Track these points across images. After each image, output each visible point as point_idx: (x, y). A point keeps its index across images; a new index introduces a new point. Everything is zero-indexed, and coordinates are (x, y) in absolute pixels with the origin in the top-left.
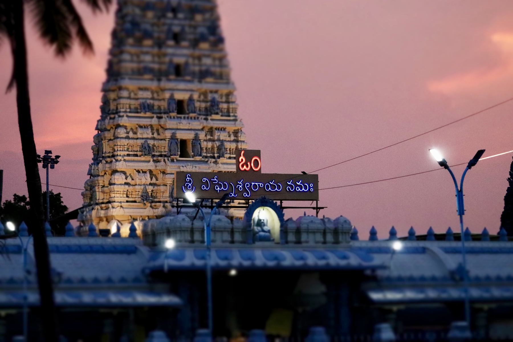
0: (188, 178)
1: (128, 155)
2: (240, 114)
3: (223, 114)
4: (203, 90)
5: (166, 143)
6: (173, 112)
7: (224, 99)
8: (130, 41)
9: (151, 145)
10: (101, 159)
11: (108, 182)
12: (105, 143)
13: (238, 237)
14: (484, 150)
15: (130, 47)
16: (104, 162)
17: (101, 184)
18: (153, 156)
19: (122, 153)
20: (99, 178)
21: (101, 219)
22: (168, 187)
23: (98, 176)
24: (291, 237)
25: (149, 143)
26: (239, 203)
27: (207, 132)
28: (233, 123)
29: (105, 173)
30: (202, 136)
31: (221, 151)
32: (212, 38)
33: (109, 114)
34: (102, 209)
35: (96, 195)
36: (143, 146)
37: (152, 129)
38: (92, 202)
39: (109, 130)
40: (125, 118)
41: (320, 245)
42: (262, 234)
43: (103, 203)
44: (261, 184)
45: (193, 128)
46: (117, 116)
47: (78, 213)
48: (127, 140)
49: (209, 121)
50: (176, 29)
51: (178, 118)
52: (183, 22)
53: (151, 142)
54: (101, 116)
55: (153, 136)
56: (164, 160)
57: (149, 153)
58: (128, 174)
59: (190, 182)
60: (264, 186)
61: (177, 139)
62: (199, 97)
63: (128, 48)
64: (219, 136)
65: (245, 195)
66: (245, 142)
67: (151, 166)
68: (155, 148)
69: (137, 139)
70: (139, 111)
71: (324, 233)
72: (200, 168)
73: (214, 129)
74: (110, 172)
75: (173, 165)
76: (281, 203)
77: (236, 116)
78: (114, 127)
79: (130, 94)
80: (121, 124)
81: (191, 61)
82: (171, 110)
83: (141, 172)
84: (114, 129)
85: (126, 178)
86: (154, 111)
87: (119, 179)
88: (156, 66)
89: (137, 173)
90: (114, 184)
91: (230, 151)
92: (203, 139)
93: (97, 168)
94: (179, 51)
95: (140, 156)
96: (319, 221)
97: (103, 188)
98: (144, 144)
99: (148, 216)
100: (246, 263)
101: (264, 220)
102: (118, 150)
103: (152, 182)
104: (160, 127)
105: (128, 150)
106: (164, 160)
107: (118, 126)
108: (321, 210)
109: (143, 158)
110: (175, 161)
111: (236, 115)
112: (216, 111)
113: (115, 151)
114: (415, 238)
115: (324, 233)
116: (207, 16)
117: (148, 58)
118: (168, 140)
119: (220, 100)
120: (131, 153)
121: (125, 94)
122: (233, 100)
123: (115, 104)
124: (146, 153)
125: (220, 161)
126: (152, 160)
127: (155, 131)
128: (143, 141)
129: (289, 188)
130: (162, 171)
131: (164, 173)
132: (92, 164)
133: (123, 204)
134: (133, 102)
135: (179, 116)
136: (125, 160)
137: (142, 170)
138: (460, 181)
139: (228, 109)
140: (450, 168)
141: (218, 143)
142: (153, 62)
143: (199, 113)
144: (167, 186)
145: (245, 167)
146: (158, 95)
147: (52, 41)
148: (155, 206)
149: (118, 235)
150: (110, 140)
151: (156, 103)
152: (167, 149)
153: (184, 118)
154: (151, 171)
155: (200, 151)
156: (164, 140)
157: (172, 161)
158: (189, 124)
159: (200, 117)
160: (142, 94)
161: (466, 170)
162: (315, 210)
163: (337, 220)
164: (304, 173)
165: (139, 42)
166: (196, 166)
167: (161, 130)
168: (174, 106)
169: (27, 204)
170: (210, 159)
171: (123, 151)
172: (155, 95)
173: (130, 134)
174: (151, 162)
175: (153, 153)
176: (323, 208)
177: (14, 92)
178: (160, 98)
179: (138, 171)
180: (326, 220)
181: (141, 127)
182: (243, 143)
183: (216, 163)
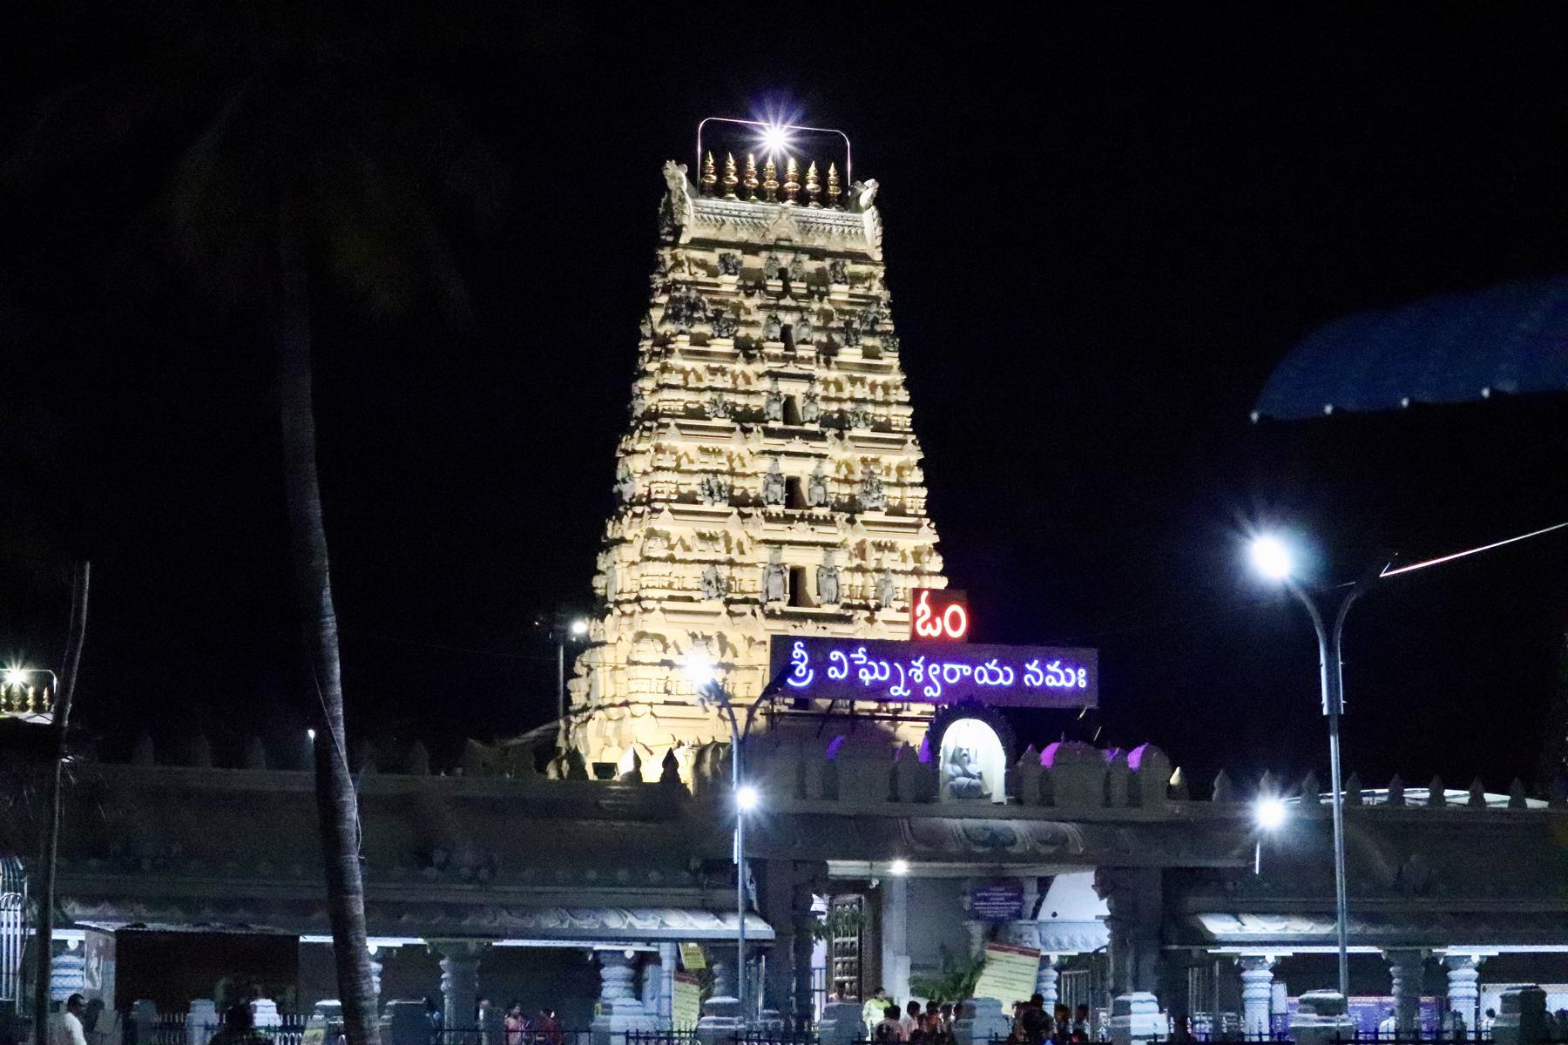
1: (672, 598)
5: (758, 574)
6: (776, 503)
10: (611, 606)
11: (625, 661)
16: (617, 612)
18: (728, 602)
23: (602, 644)
25: (719, 571)
26: (922, 713)
28: (914, 530)
33: (632, 505)
40: (666, 514)
42: (964, 780)
43: (612, 705)
49: (859, 524)
50: (788, 319)
53: (724, 572)
55: (728, 556)
58: (669, 641)
59: (802, 659)
62: (838, 471)
68: (733, 583)
70: (699, 498)
79: (678, 460)
80: (657, 528)
85: (665, 651)
88: (741, 400)
89: (690, 638)
92: (844, 566)
95: (699, 601)
102: (647, 587)
103: (724, 660)
105: (670, 586)
106: (754, 614)
107: (651, 534)
112: (875, 504)
116: (860, 289)
118: (763, 565)
119: (884, 479)
123: (647, 484)
126: (724, 610)
127: (734, 544)
129: (1029, 680)
130: (747, 637)
133: (656, 709)
135: (789, 511)
136: (664, 611)
150: (633, 563)
151: (738, 482)
152: (759, 587)
153: (802, 519)
158: (813, 529)
167: (746, 546)
168: (779, 491)
171: (659, 588)
173: (675, 549)
174: (721, 616)
175: (729, 596)
178: (748, 471)
179: (694, 636)
183: (871, 620)
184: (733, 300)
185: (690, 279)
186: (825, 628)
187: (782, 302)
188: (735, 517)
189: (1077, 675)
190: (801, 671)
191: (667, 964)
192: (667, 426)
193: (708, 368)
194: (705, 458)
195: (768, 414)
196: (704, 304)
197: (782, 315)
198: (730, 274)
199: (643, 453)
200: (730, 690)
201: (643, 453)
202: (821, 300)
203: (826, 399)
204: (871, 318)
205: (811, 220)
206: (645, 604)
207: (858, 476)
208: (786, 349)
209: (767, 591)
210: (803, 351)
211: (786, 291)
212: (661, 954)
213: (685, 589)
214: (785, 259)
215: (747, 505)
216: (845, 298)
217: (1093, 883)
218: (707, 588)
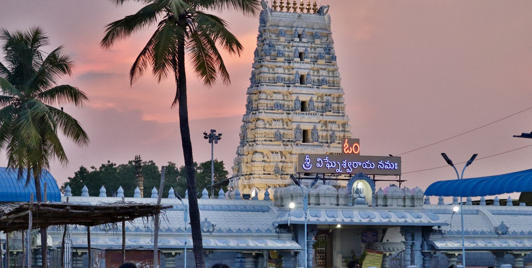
0: (307, 158)
1: (265, 140)
2: (347, 111)
3: (335, 111)
4: (321, 94)
5: (292, 132)
6: (298, 109)
7: (335, 101)
8: (268, 58)
9: (281, 134)
10: (246, 143)
11: (250, 160)
12: (249, 131)
13: (341, 201)
14: (477, 154)
15: (267, 63)
17: (246, 161)
19: (261, 139)
20: (244, 157)
21: (245, 187)
22: (294, 164)
23: (244, 155)
24: (380, 202)
27: (323, 124)
28: (342, 118)
29: (249, 153)
30: (319, 127)
31: (332, 139)
32: (327, 56)
34: (246, 179)
35: (242, 169)
36: (276, 134)
37: (283, 122)
38: (239, 174)
39: (252, 122)
40: (263, 113)
41: (401, 207)
43: (246, 175)
44: (359, 163)
45: (312, 121)
46: (257, 112)
47: (229, 181)
48: (264, 129)
49: (324, 116)
50: (301, 50)
51: (302, 114)
52: (306, 45)
54: (246, 112)
56: (291, 144)
57: (280, 139)
58: (265, 154)
59: (308, 161)
60: (362, 165)
61: (301, 129)
62: (318, 99)
63: (266, 63)
64: (331, 127)
65: (348, 171)
66: (351, 131)
67: (281, 148)
68: (285, 135)
69: (272, 129)
70: (274, 108)
71: (404, 199)
72: (317, 151)
73: (328, 122)
74: (252, 152)
75: (297, 147)
76: (374, 177)
77: (344, 113)
78: (255, 120)
79: (267, 96)
80: (260, 118)
81: (311, 73)
82: (297, 109)
83: (274, 152)
84: (255, 121)
85: (263, 157)
86: (285, 109)
87: (258, 157)
88: (287, 76)
90: (255, 161)
91: (339, 138)
93: (242, 149)
94: (303, 66)
95: (274, 141)
96: (401, 191)
97: (247, 164)
98: (277, 132)
99: (279, 185)
100: (347, 220)
101: (360, 189)
102: (258, 137)
104: (288, 120)
105: (265, 137)
106: (291, 144)
107: (258, 119)
108: (402, 182)
109: (276, 143)
110: (299, 145)
111: (344, 112)
112: (330, 109)
113: (255, 137)
114: (471, 203)
115: (404, 199)
116: (324, 40)
117: (280, 70)
118: (294, 130)
119: (332, 101)
120: (267, 139)
121: (263, 96)
122: (342, 101)
124: (278, 139)
125: (331, 145)
126: (282, 144)
127: (285, 123)
128: (276, 130)
129: (379, 166)
131: (291, 153)
132: (240, 146)
134: (269, 102)
135: (302, 112)
137: (275, 151)
138: (461, 175)
139: (338, 108)
140: (454, 166)
141: (330, 133)
142: (284, 74)
143: (317, 110)
144: (292, 163)
145: (348, 151)
146: (288, 98)
147: (203, 74)
148: (284, 177)
149: (256, 198)
150: (253, 129)
152: (293, 136)
153: (306, 114)
154: (281, 152)
155: (317, 137)
156: (292, 129)
157: (297, 145)
158: (310, 118)
159: (318, 113)
160: (275, 96)
161: (465, 167)
162: (399, 182)
163: (414, 189)
164: (391, 155)
165: (274, 60)
166: (315, 149)
167: (289, 123)
168: (299, 105)
169: (199, 168)
170: (325, 144)
172: (285, 97)
175: (283, 139)
176: (404, 181)
177: (177, 105)
179: (272, 152)
180: (406, 190)
181: (275, 120)
182: (348, 133)
183: (329, 146)
184: (284, 44)
185: (270, 38)
186: (314, 150)
187: (299, 45)
188: (285, 115)
189: (395, 165)
190: (308, 165)
191: (266, 257)
192: (264, 85)
193: (276, 66)
194: (275, 95)
195: (295, 81)
196: (275, 46)
197: (299, 48)
198: (282, 36)
199: (255, 94)
200: (284, 170)
201: (255, 94)
202: (312, 44)
203: (314, 76)
204: (328, 48)
205: (308, 18)
206: (256, 142)
207: (325, 100)
208: (301, 60)
209: (296, 138)
210: (306, 60)
211: (300, 40)
212: (264, 254)
213: (269, 138)
214: (300, 30)
215: (289, 111)
216: (319, 43)
217: (400, 231)
218: (276, 137)
